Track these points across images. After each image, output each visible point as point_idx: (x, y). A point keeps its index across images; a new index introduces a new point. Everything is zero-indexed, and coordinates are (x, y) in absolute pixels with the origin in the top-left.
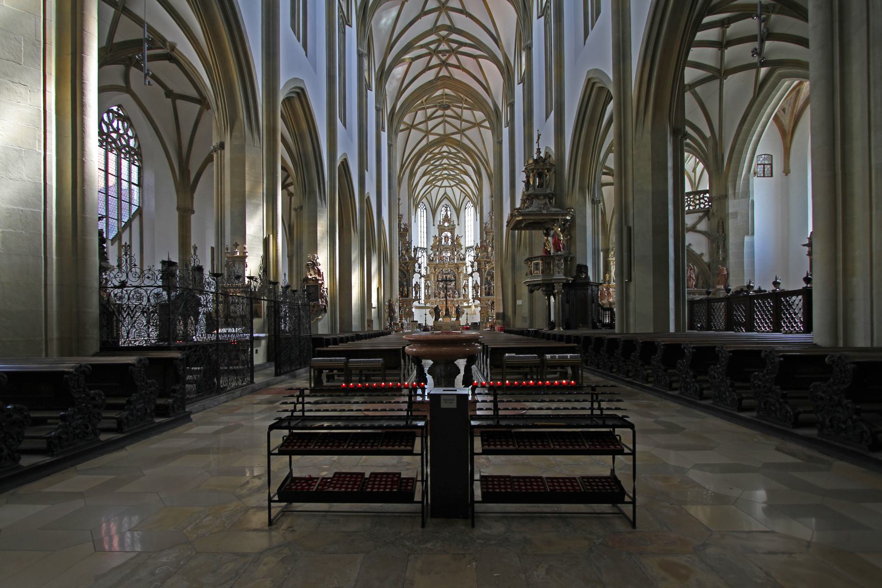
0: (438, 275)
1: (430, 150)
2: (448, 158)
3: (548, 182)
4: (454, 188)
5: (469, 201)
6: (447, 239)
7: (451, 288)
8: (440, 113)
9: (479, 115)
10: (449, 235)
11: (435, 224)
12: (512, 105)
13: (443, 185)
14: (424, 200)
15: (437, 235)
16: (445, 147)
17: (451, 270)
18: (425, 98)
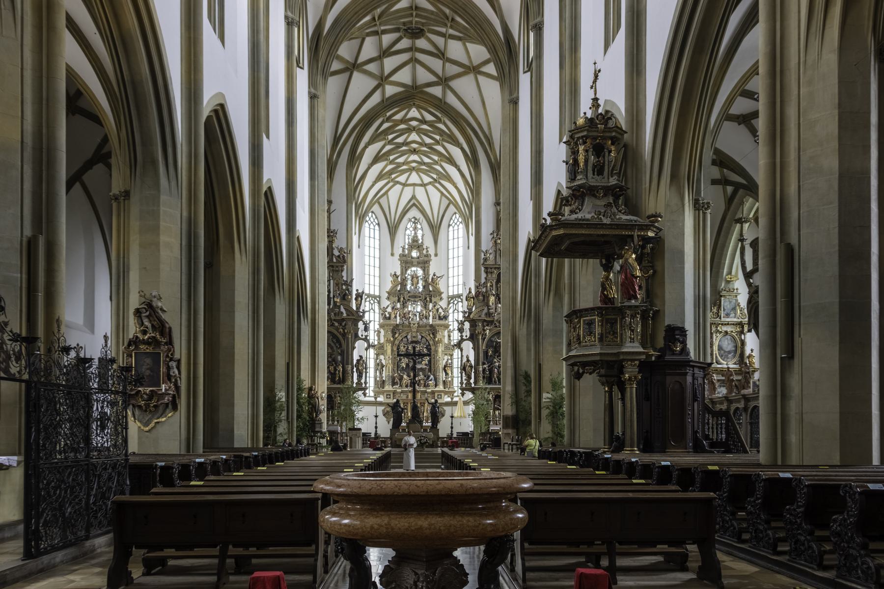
0: (399, 346)
1: (388, 114)
2: (419, 131)
3: (613, 163)
4: (430, 188)
5: (455, 213)
6: (415, 279)
7: (422, 369)
8: (405, 43)
9: (478, 52)
10: (420, 272)
11: (395, 252)
12: (539, 29)
13: (408, 183)
14: (376, 208)
15: (398, 273)
16: (414, 109)
18: (379, 10)
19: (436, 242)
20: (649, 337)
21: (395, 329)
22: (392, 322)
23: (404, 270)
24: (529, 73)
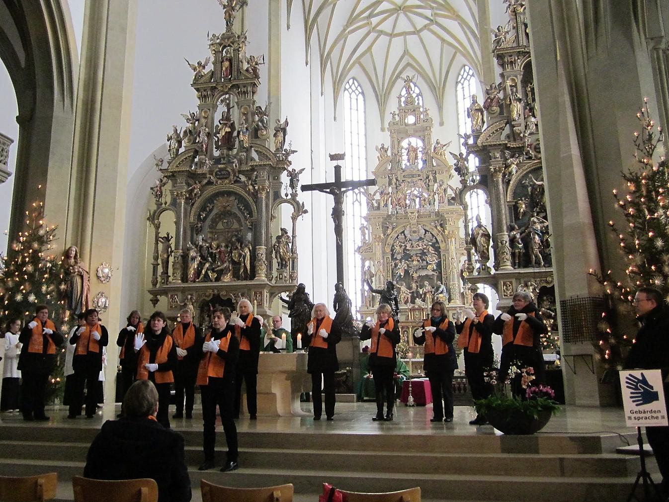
0: (393, 246)
5: (464, 66)
10: (416, 142)
14: (356, 71)
15: (387, 144)
17: (426, 231)
19: (440, 108)
21: (386, 223)
22: (383, 212)
23: (396, 142)
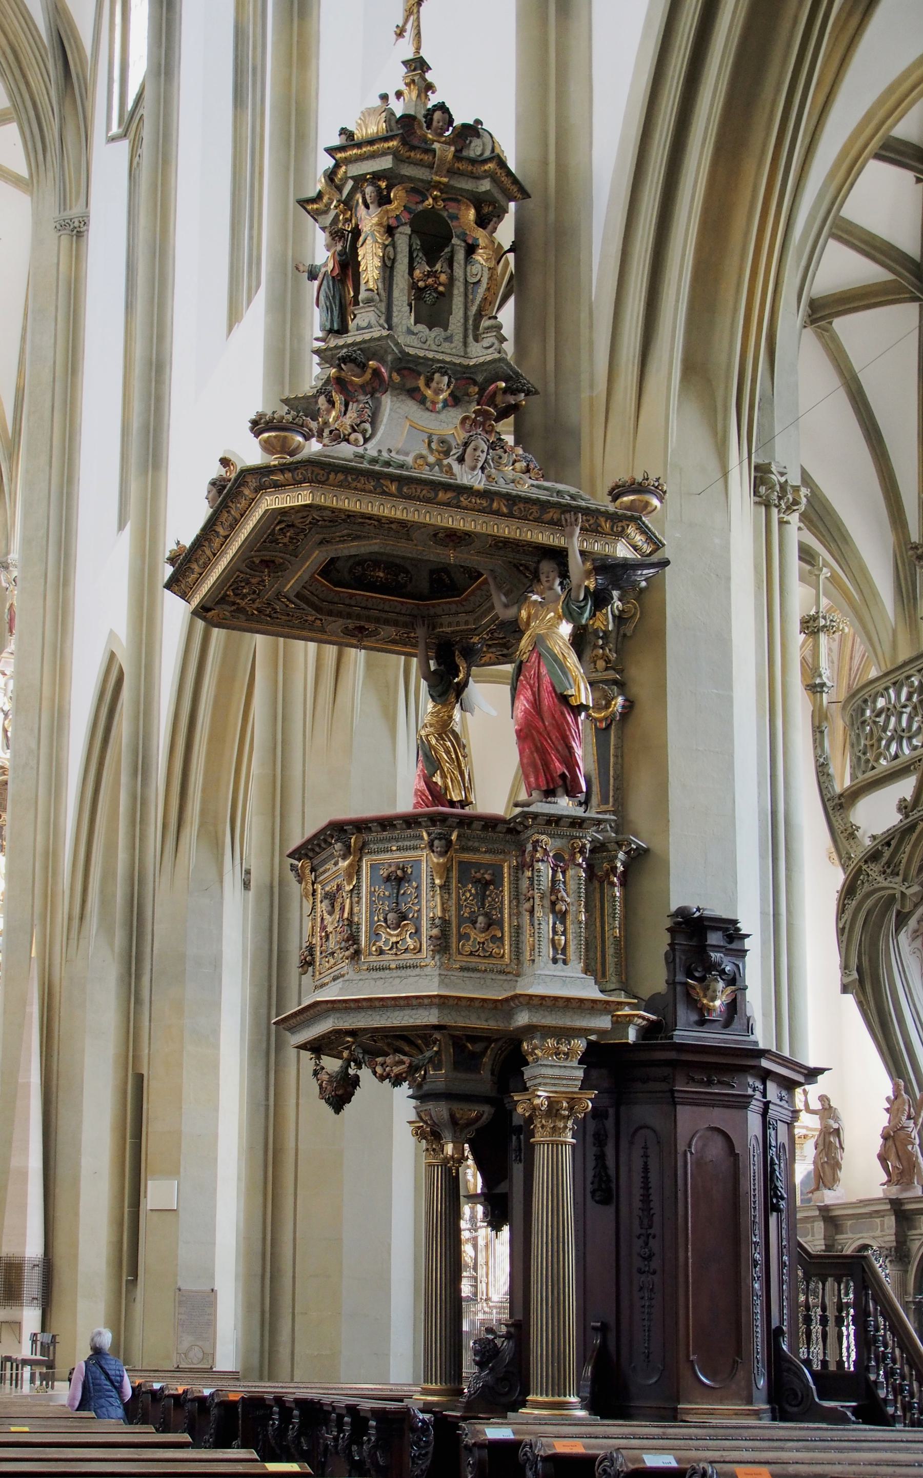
3: (481, 290)
20: (610, 951)
24: (124, 145)
